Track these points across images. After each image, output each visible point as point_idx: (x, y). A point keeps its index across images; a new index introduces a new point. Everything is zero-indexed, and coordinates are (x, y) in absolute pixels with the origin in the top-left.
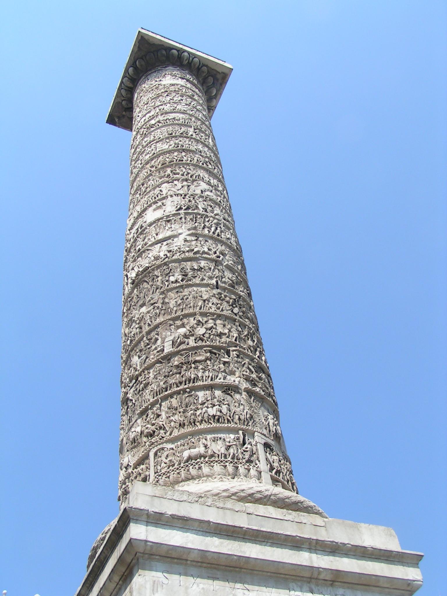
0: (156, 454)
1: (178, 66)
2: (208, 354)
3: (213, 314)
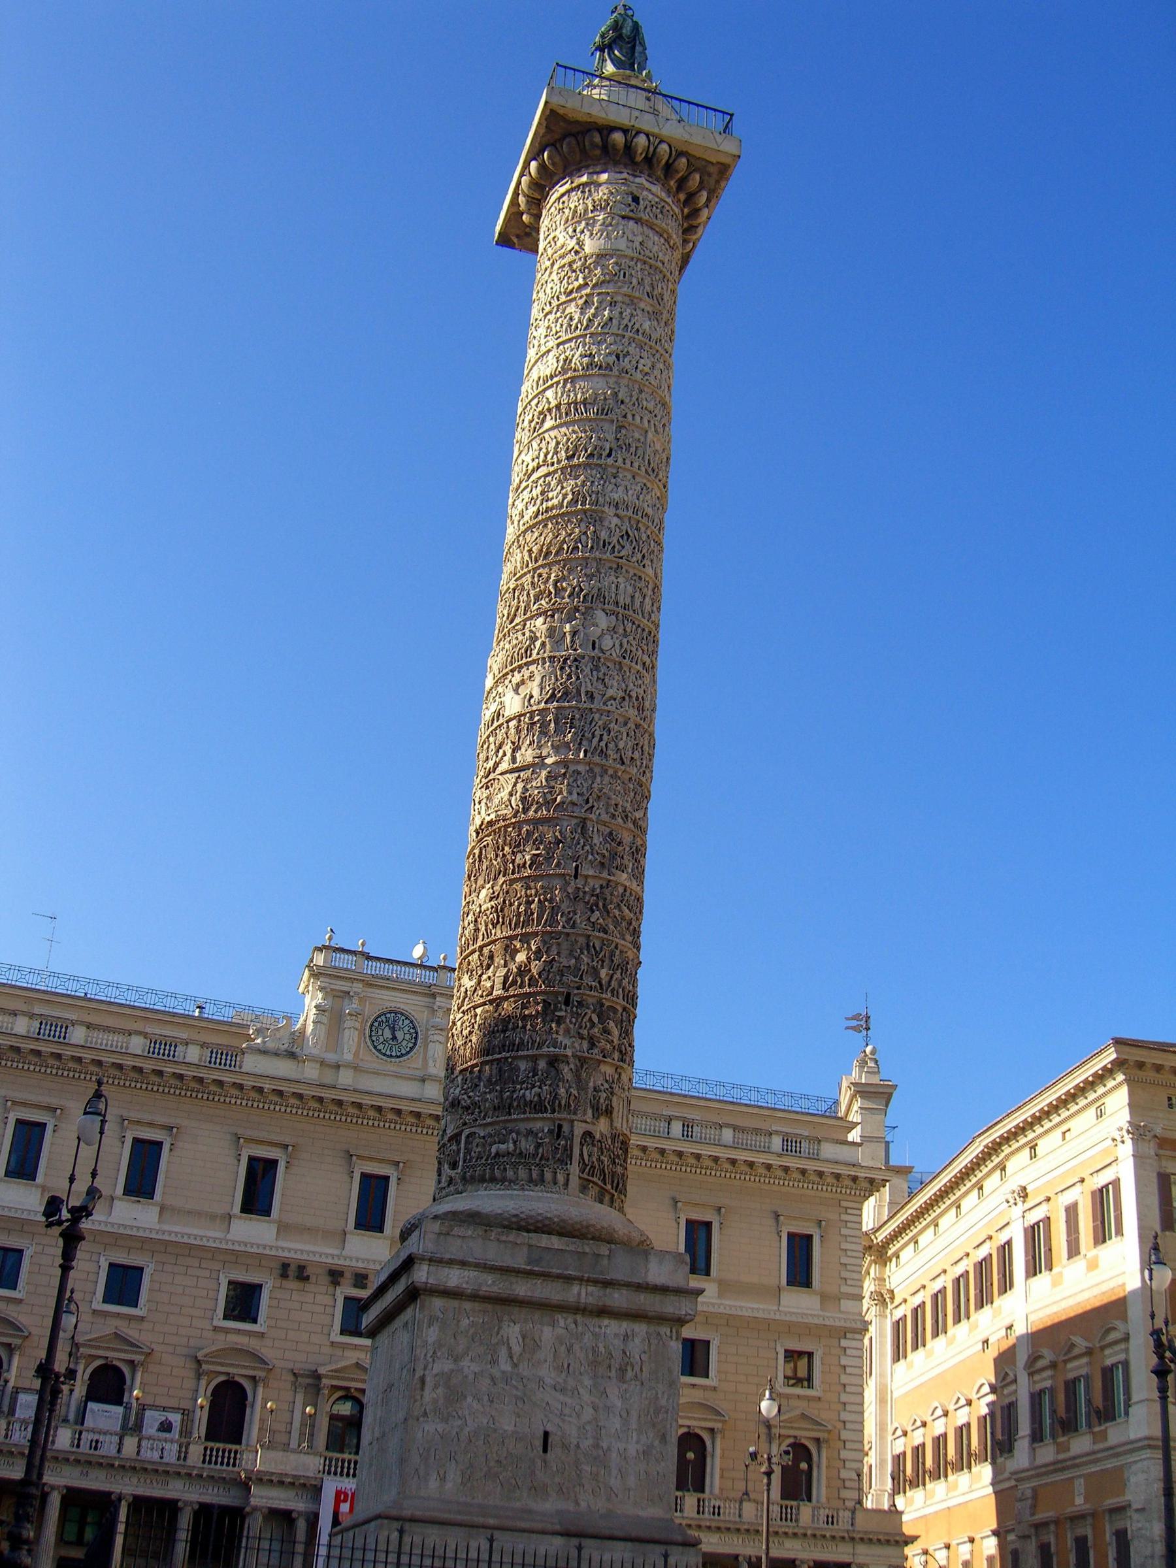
0: (468, 1137)
1: (626, 166)
3: (560, 933)
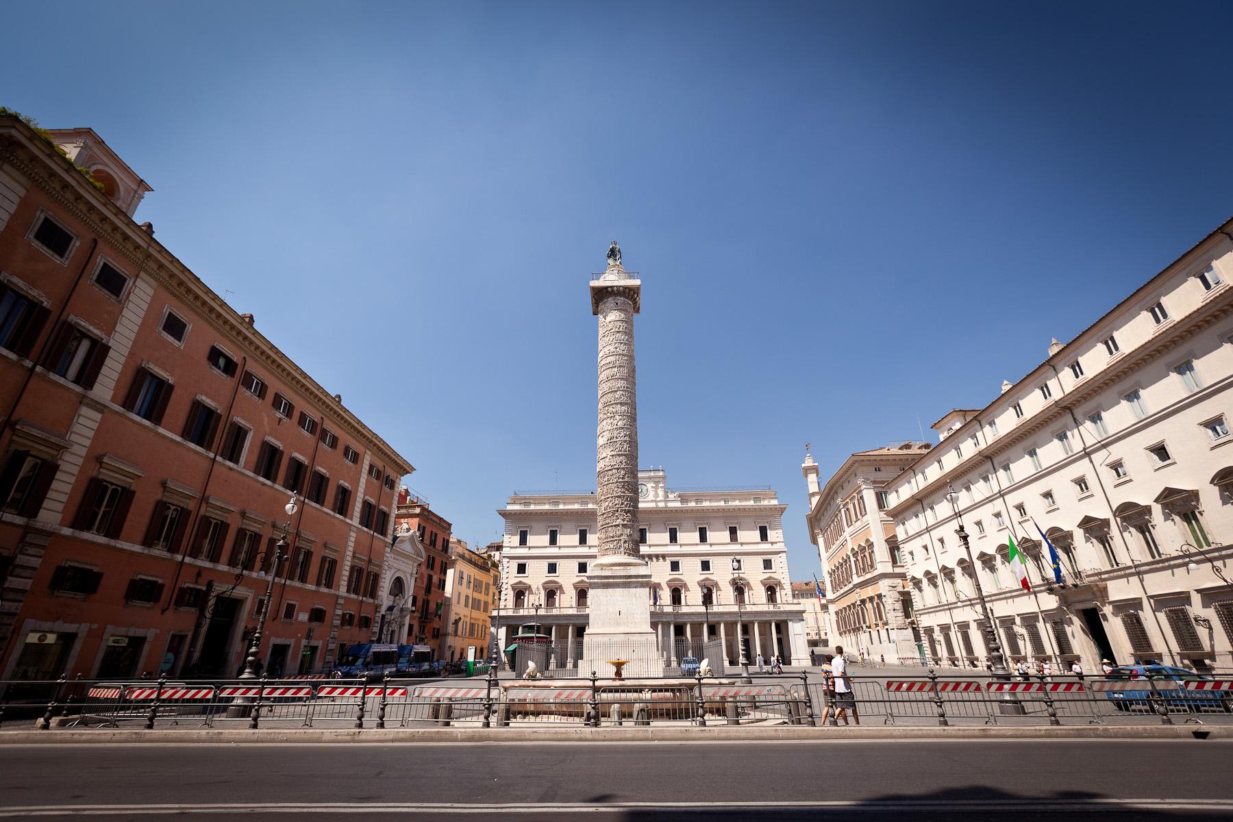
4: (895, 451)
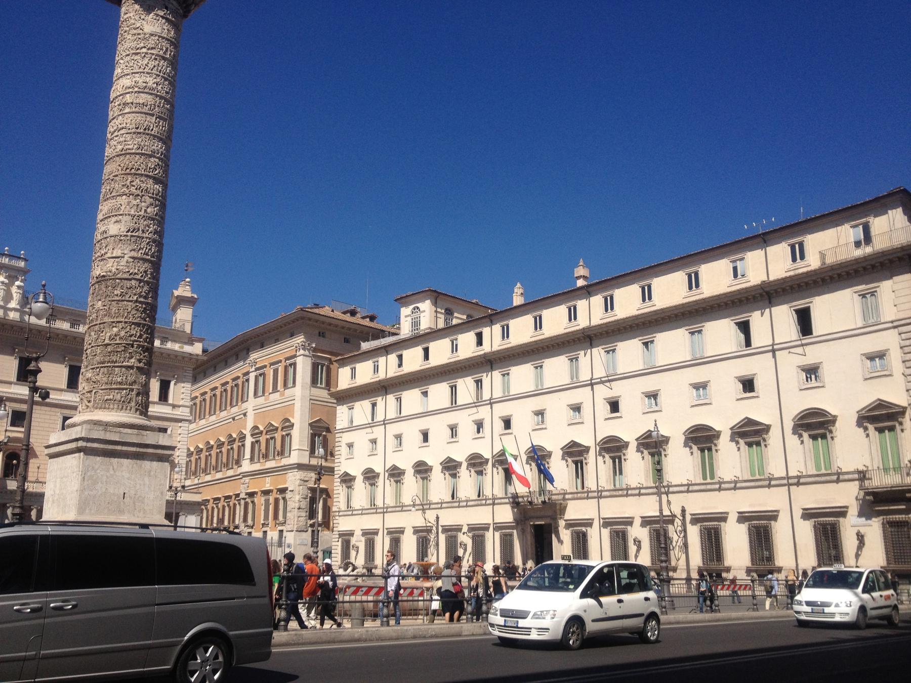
0: (95, 393)
2: (123, 348)
3: (130, 322)
4: (338, 314)
